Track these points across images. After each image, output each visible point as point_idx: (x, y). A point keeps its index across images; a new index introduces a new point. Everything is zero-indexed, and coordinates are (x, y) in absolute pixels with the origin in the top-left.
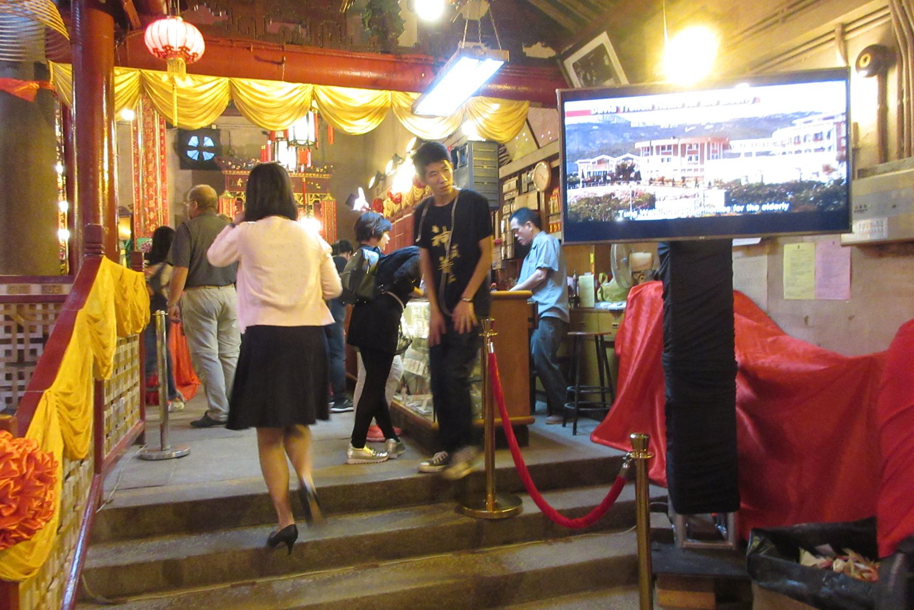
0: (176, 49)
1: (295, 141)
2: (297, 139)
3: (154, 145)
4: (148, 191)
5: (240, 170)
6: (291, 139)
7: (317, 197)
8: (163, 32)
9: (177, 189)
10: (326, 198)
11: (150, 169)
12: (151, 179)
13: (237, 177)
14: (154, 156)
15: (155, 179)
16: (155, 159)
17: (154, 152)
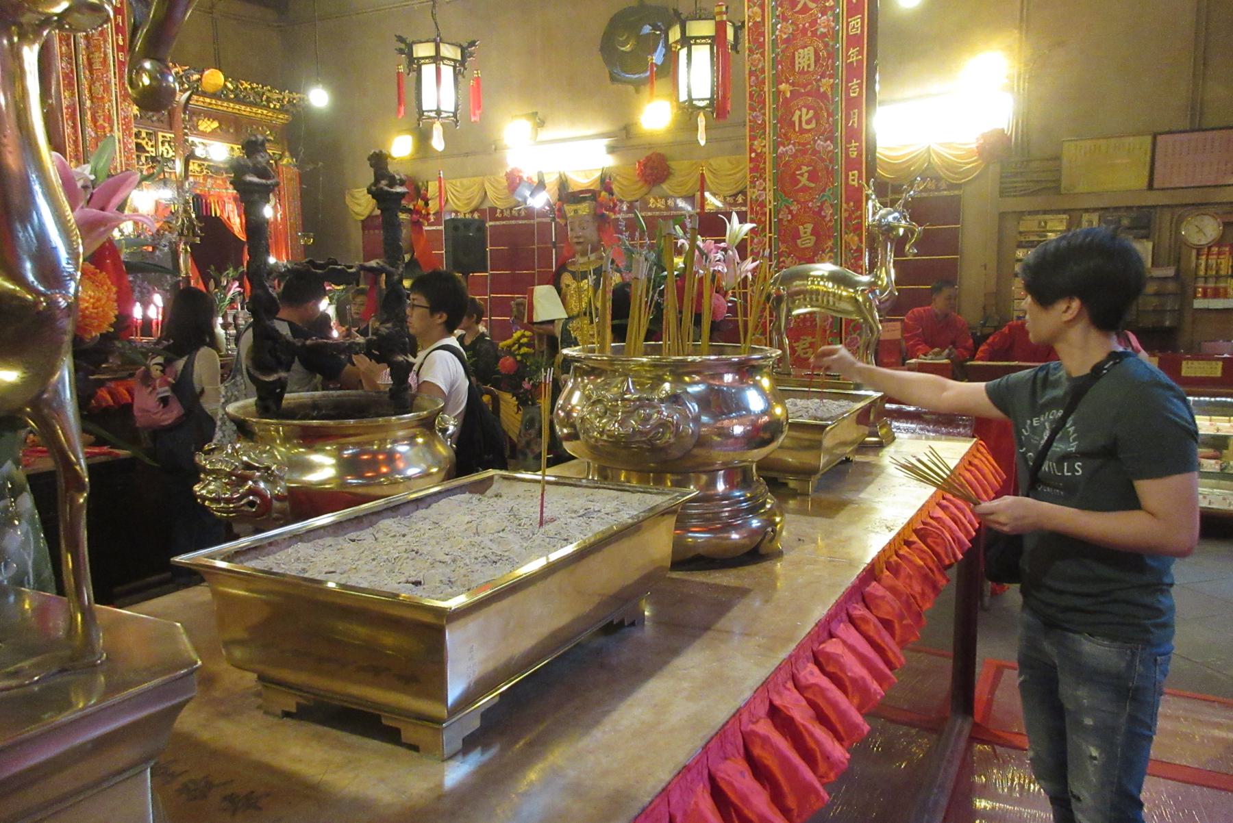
10: (285, 162)
11: (97, 66)
16: (105, 41)
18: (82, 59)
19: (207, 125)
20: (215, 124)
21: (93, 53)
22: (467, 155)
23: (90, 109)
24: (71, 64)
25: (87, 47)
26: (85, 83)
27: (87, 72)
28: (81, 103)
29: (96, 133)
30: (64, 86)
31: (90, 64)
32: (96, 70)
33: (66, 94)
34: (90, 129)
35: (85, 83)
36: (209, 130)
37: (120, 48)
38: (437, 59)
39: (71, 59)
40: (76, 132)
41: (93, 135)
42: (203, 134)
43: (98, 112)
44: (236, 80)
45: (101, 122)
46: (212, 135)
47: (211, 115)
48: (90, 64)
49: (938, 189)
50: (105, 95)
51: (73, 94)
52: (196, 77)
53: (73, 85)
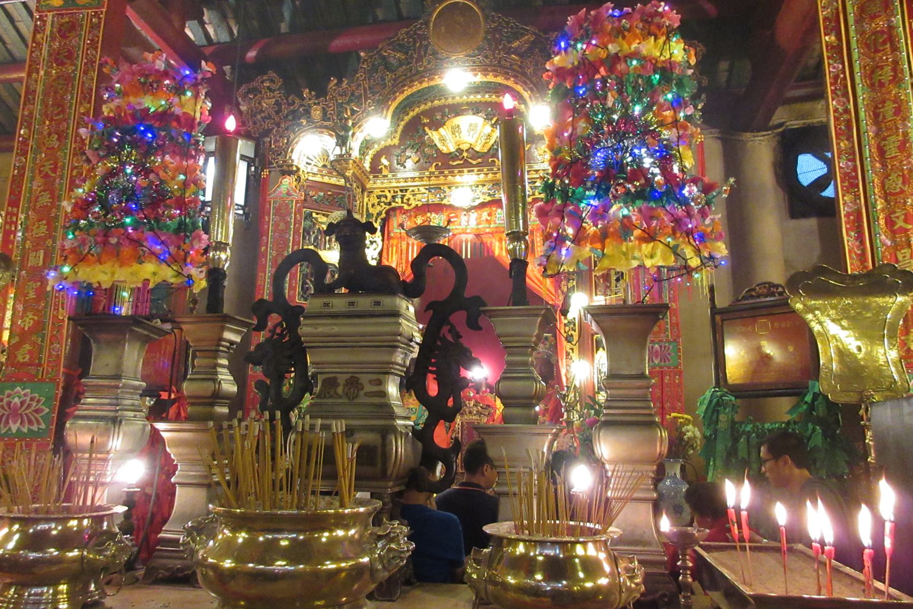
4: (890, 223)
21: (884, 139)
23: (883, 210)
24: (854, 160)
25: (877, 135)
26: (874, 179)
27: (878, 165)
29: (893, 240)
30: (842, 189)
31: (882, 152)
32: (892, 158)
33: (845, 198)
34: (883, 237)
35: (874, 179)
39: (854, 154)
40: (862, 242)
41: (889, 243)
43: (895, 212)
45: (900, 223)
50: (906, 188)
51: (857, 197)
53: (857, 186)
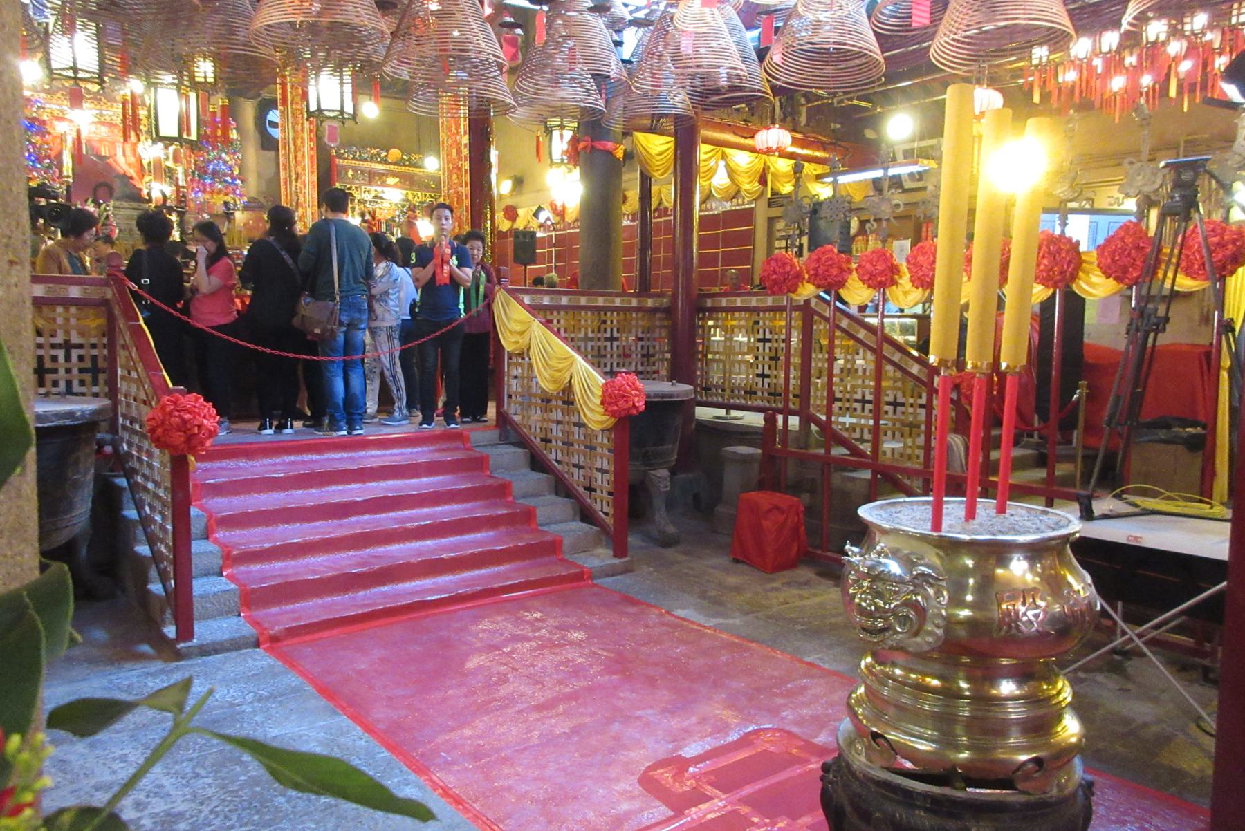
0: (774, 148)
1: (320, 110)
2: (323, 108)
3: (302, 130)
5: (354, 159)
6: (313, 107)
7: (432, 197)
8: (764, 138)
9: (259, 175)
11: (299, 158)
12: (299, 169)
13: (346, 168)
14: (303, 143)
15: (304, 170)
16: (304, 147)
17: (302, 138)
18: (292, 156)
19: (391, 181)
20: (397, 180)
22: (538, 191)
28: (290, 176)
31: (296, 157)
36: (392, 183)
37: (312, 149)
38: (562, 127)
42: (389, 186)
44: (409, 154)
46: (395, 186)
47: (394, 174)
48: (296, 157)
49: (743, 204)
52: (384, 154)
